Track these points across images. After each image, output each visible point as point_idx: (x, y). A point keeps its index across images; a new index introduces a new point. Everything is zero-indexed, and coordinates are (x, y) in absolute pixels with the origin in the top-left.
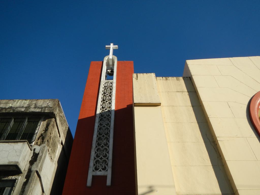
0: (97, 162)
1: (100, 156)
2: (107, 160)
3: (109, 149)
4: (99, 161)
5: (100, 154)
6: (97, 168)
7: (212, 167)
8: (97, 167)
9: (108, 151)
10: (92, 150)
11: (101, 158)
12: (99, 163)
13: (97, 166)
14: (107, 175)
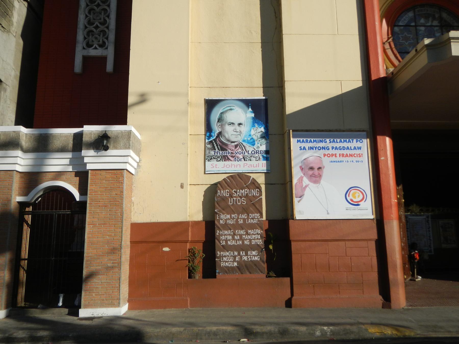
0: (90, 33)
1: (95, 22)
2: (107, 30)
3: (110, 9)
4: (92, 31)
5: (94, 19)
6: (90, 43)
7: (260, 45)
8: (90, 41)
9: (109, 14)
10: (80, 12)
11: (97, 27)
12: (93, 35)
13: (89, 40)
14: (107, 56)
